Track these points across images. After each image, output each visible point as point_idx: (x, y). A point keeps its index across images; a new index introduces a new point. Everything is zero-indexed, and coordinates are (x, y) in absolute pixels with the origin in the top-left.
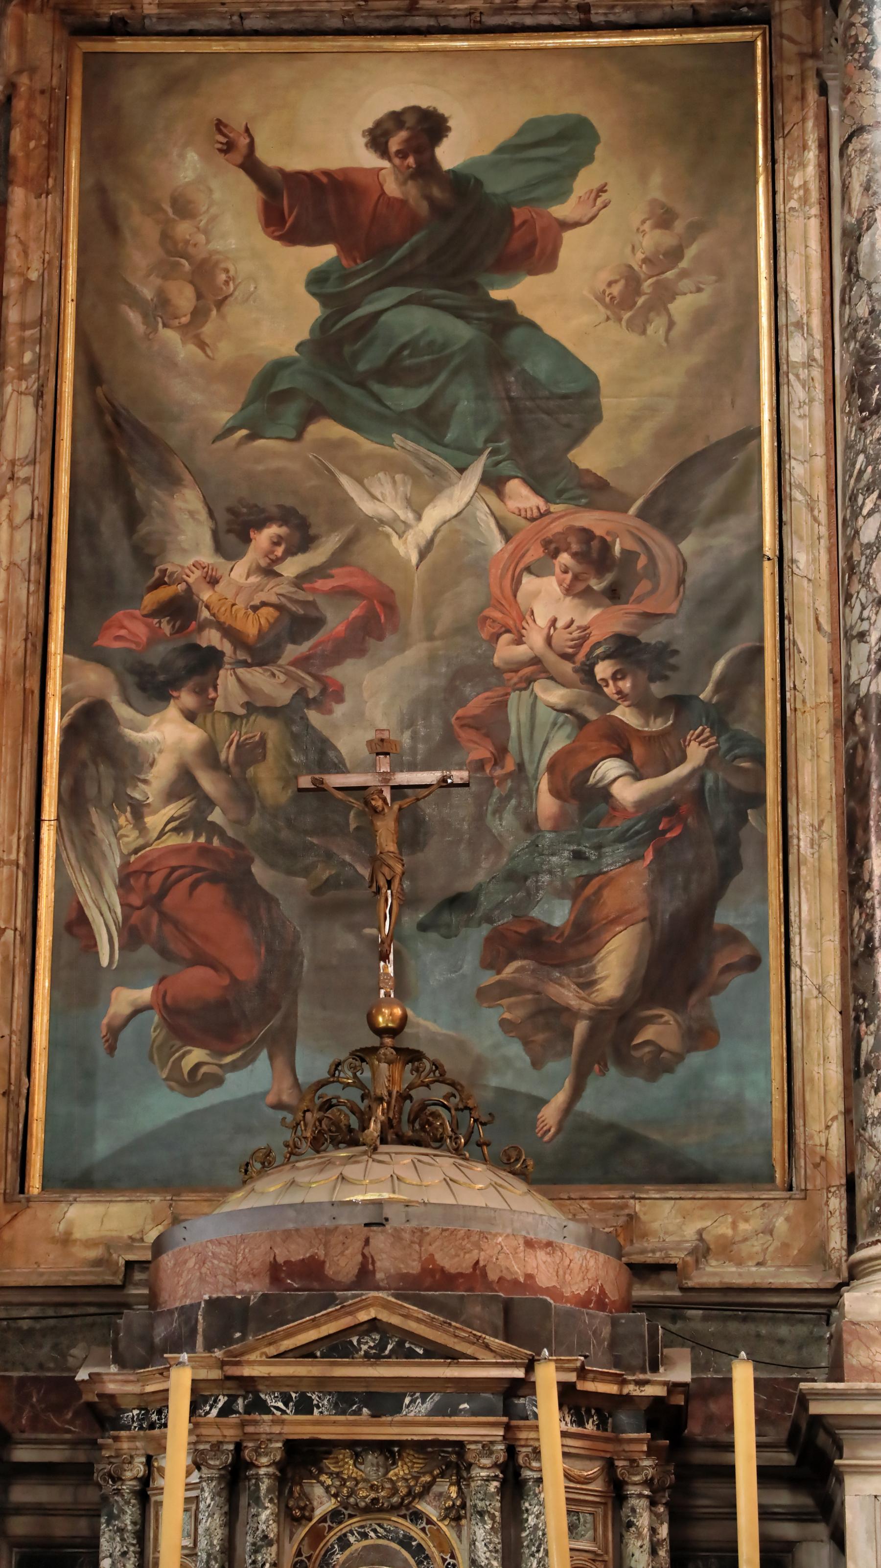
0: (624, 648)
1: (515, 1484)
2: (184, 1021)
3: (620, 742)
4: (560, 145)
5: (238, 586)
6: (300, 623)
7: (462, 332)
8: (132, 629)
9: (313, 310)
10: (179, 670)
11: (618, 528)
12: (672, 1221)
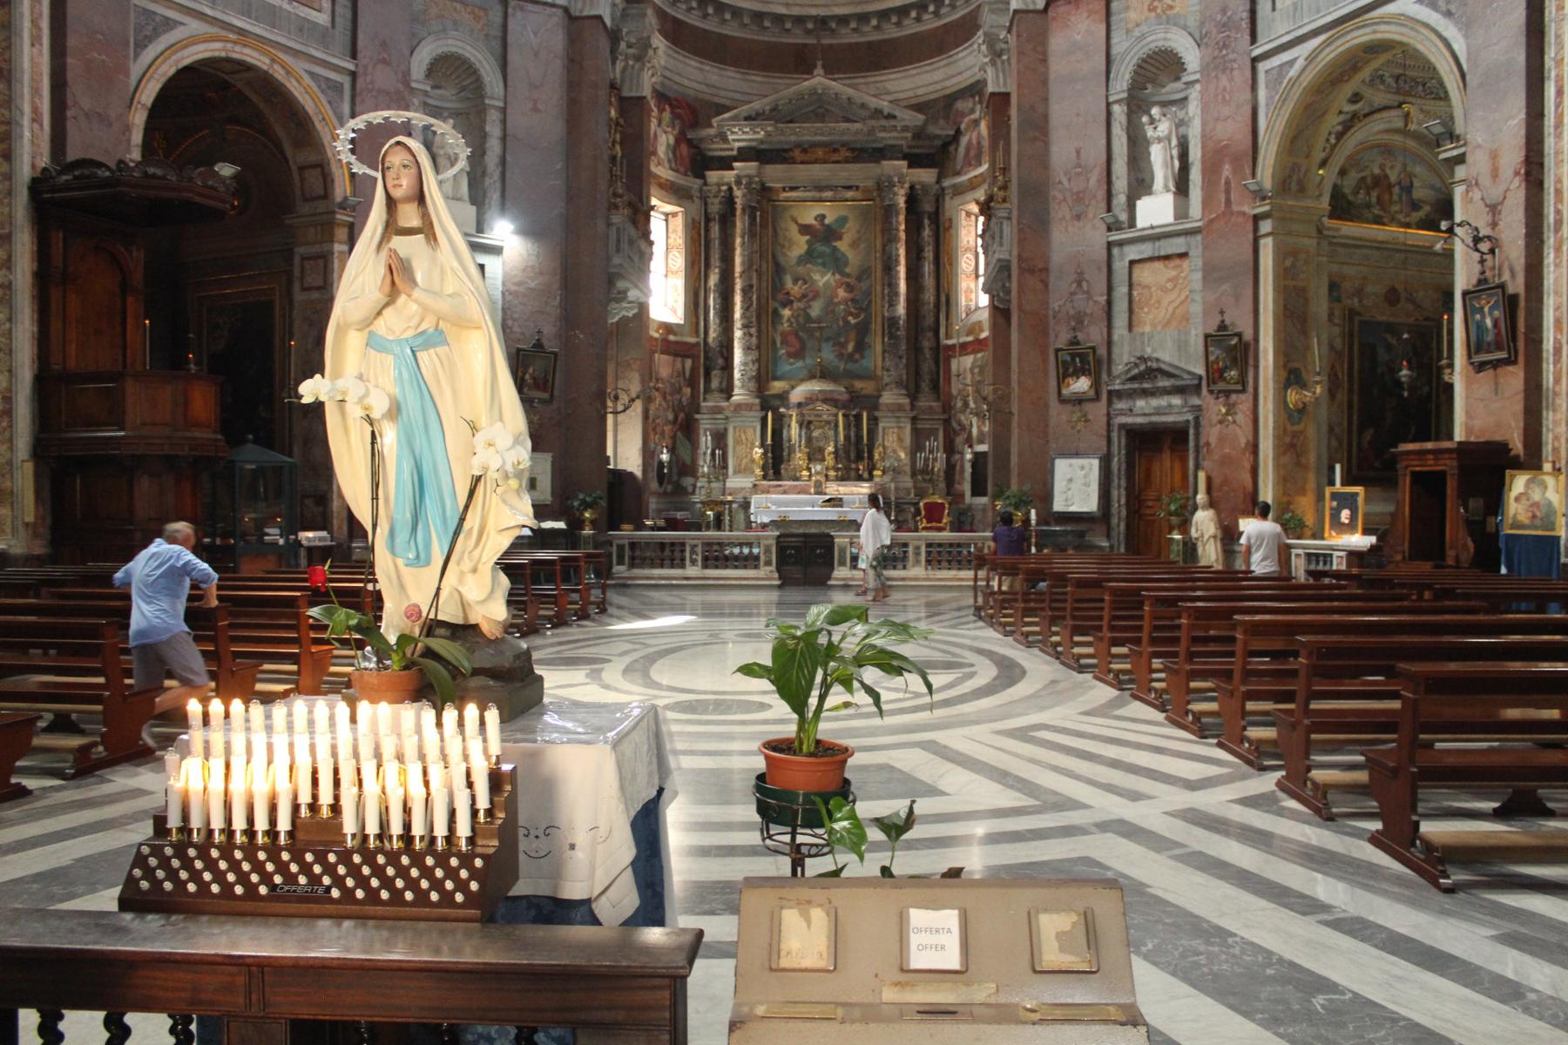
0: (852, 300)
1: (836, 426)
2: (789, 355)
3: (851, 314)
4: (843, 220)
5: (795, 290)
6: (804, 296)
7: (828, 250)
8: (780, 297)
9: (806, 247)
10: (787, 303)
11: (851, 281)
12: (858, 385)
